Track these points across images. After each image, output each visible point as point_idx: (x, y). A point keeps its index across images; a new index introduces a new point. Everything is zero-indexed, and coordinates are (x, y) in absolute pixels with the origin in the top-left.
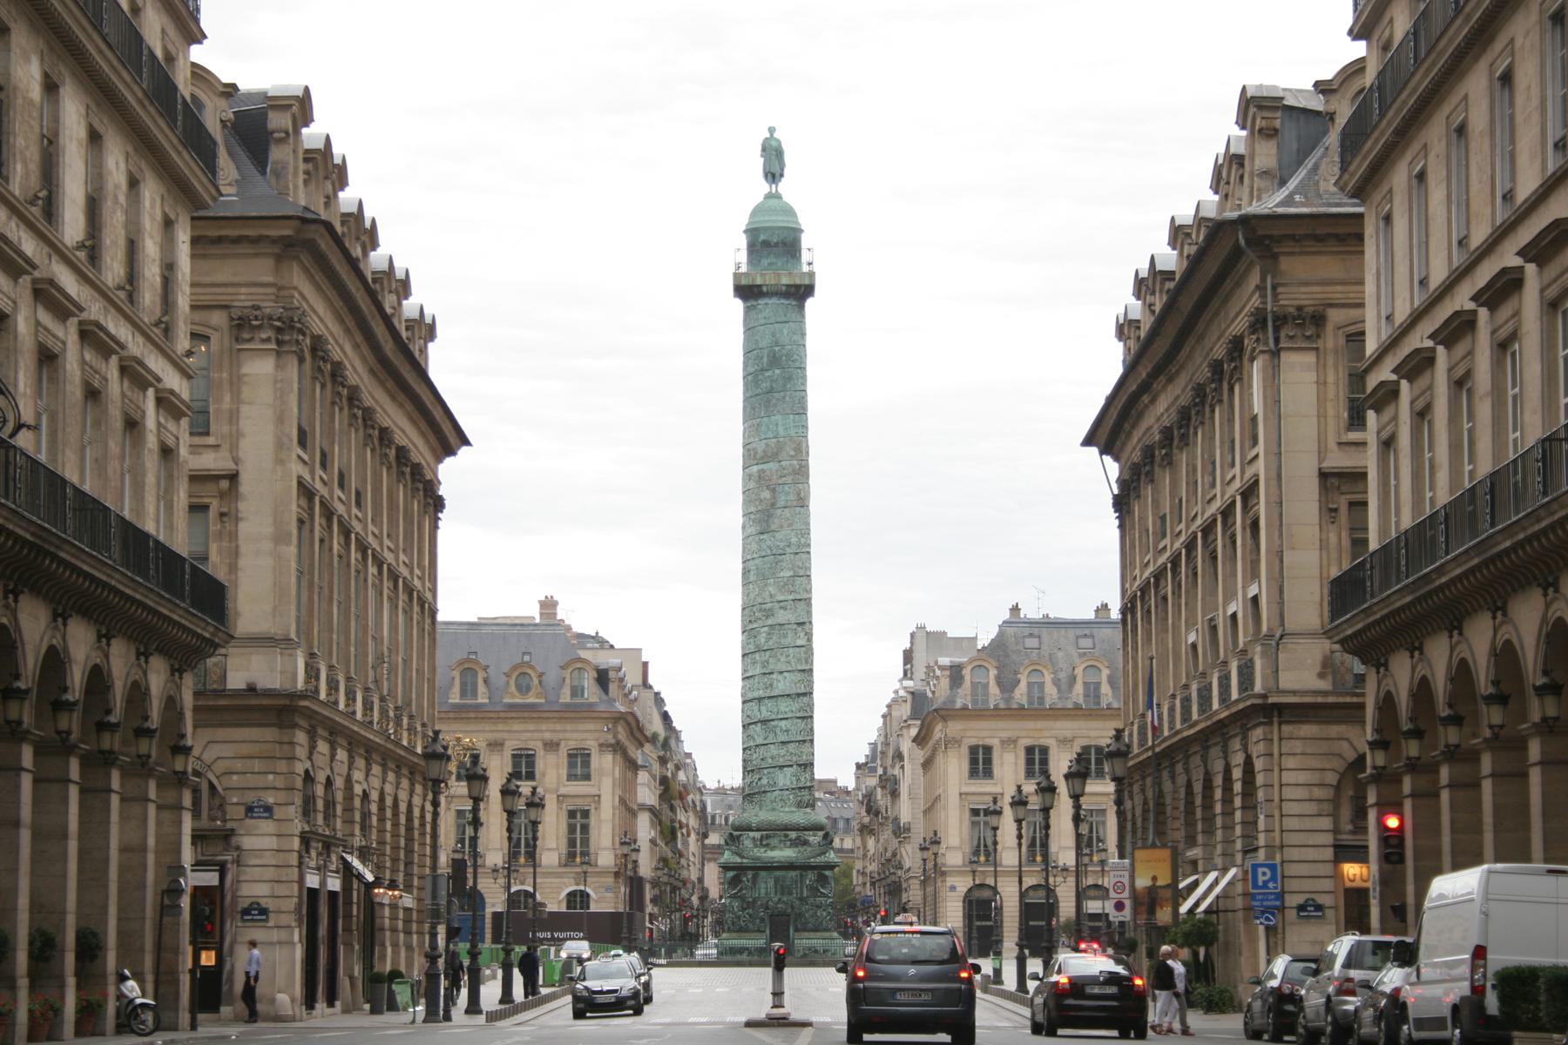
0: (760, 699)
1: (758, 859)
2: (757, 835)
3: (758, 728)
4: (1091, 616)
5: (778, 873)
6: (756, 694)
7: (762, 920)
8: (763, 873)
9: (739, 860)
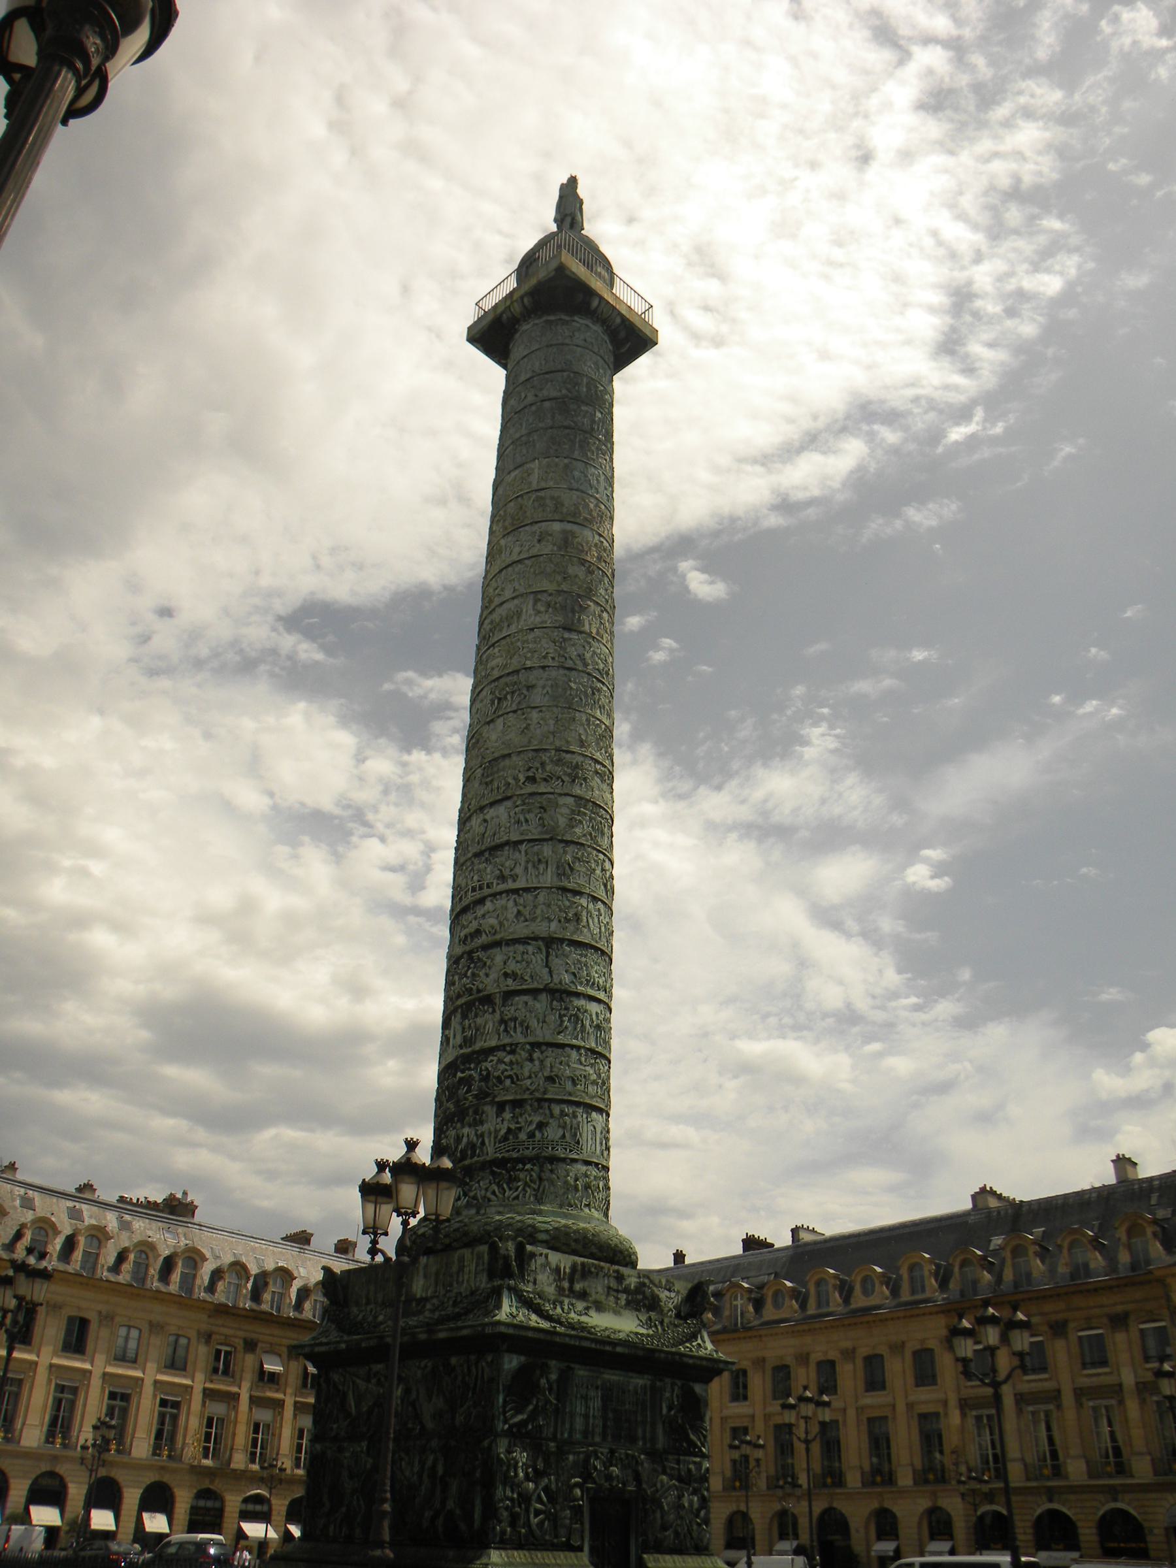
0: (551, 943)
1: (583, 1328)
2: (562, 1261)
3: (541, 1004)
4: (72, 1190)
5: (612, 1376)
6: (542, 928)
7: (577, 1511)
8: (581, 1372)
9: (545, 1325)
